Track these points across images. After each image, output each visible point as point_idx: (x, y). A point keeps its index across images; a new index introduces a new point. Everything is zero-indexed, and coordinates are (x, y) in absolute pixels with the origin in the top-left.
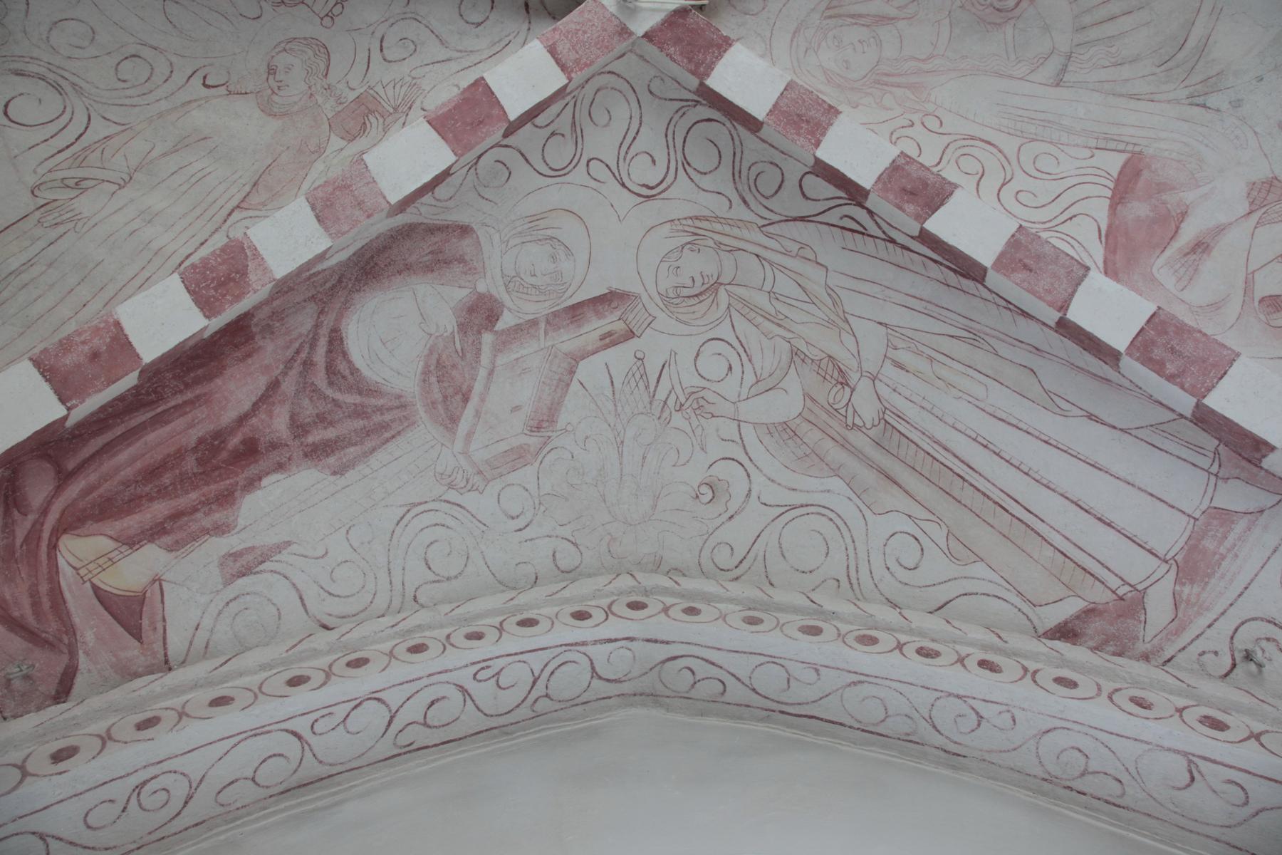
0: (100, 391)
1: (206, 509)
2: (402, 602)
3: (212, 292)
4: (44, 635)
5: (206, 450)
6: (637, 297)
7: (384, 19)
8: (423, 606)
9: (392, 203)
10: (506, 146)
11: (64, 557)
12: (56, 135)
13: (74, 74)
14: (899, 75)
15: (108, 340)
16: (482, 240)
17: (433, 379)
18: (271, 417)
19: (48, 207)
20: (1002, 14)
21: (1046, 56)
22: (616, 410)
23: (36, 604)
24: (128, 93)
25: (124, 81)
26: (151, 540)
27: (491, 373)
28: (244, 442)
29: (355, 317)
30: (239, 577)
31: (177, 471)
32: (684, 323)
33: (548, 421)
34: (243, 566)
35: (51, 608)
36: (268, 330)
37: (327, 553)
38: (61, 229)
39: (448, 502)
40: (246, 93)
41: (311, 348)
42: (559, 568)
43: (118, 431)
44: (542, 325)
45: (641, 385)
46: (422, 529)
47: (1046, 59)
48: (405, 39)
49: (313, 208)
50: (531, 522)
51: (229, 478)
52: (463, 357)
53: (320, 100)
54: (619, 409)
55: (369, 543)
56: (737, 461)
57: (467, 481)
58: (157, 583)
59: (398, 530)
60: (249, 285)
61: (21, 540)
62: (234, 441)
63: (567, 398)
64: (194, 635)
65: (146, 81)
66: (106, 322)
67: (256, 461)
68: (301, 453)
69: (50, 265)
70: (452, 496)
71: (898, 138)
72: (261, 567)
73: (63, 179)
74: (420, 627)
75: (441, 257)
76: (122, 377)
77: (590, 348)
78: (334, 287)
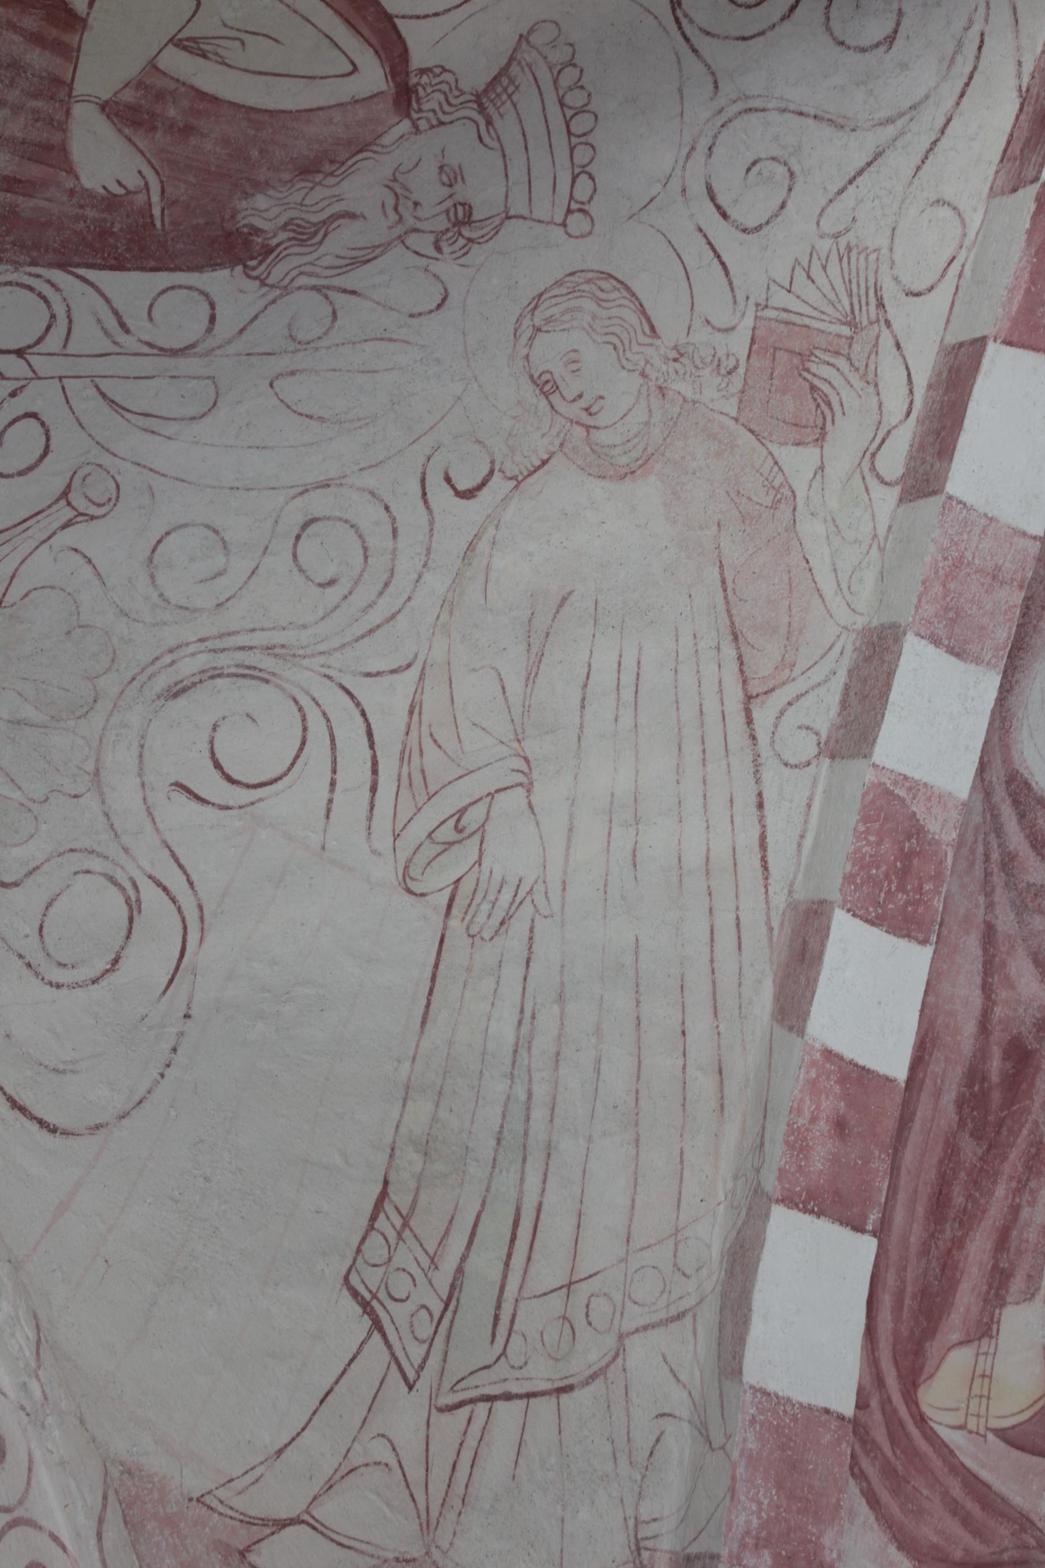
1: (1027, 1197)
4: (1006, 1556)
5: (972, 1111)
7: (685, 151)
9: (1042, 534)
11: (940, 1424)
12: (334, 762)
13: (253, 630)
15: (837, 1089)
18: (1012, 987)
19: (460, 903)
23: (966, 1521)
24: (360, 598)
25: (331, 583)
26: (1002, 1306)
28: (1006, 1056)
31: (963, 1175)
35: (983, 1509)
38: (519, 927)
40: (544, 463)
41: (998, 836)
48: (754, 163)
49: (936, 641)
51: (1023, 1126)
53: (684, 387)
60: (938, 843)
61: (889, 1445)
62: (995, 1066)
65: (366, 557)
66: (814, 1064)
69: (561, 998)
73: (430, 835)
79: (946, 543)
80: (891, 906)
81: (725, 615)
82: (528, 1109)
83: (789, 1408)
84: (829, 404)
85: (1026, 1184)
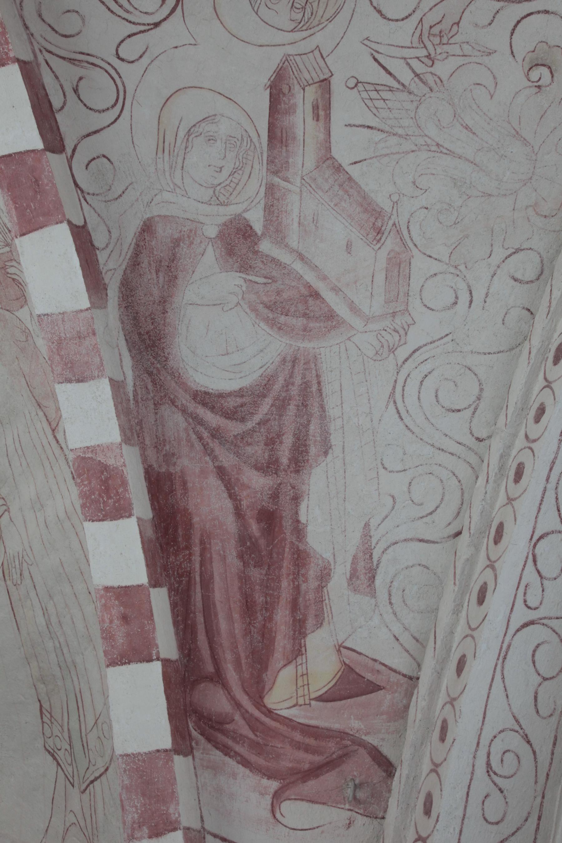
0: (154, 628)
1: (301, 579)
2: (476, 454)
3: (111, 501)
4: (334, 756)
5: (250, 556)
6: (287, 58)
8: (489, 437)
10: (74, 151)
11: (281, 709)
15: (117, 602)
16: (164, 212)
17: (282, 319)
18: (249, 488)
22: (400, 136)
23: (307, 749)
26: (305, 635)
27: (302, 257)
29: (191, 372)
30: (373, 582)
31: (257, 587)
32: (336, 13)
33: (376, 219)
34: (366, 574)
35: (316, 739)
36: (169, 458)
37: (393, 497)
38: (26, 574)
39: (406, 360)
41: (202, 425)
42: (532, 282)
43: (200, 619)
44: (276, 180)
45: (386, 95)
46: (419, 399)
49: (69, 381)
50: (469, 286)
51: (284, 548)
52: (274, 280)
54: (400, 131)
55: (405, 454)
56: (523, 18)
57: (395, 331)
58: (341, 649)
59: (407, 420)
61: (251, 733)
62: (255, 528)
63: (363, 186)
64: (402, 645)
66: (102, 597)
67: (281, 517)
68: (293, 475)
70: (402, 353)
72: (375, 559)
74: (503, 457)
75: (165, 263)
76: (151, 607)
77: (322, 136)
78: (154, 382)
79: (50, 336)
80: (108, 508)
81: (33, 398)
82: (62, 650)
83: (140, 758)
84: (20, 284)
85: (298, 574)
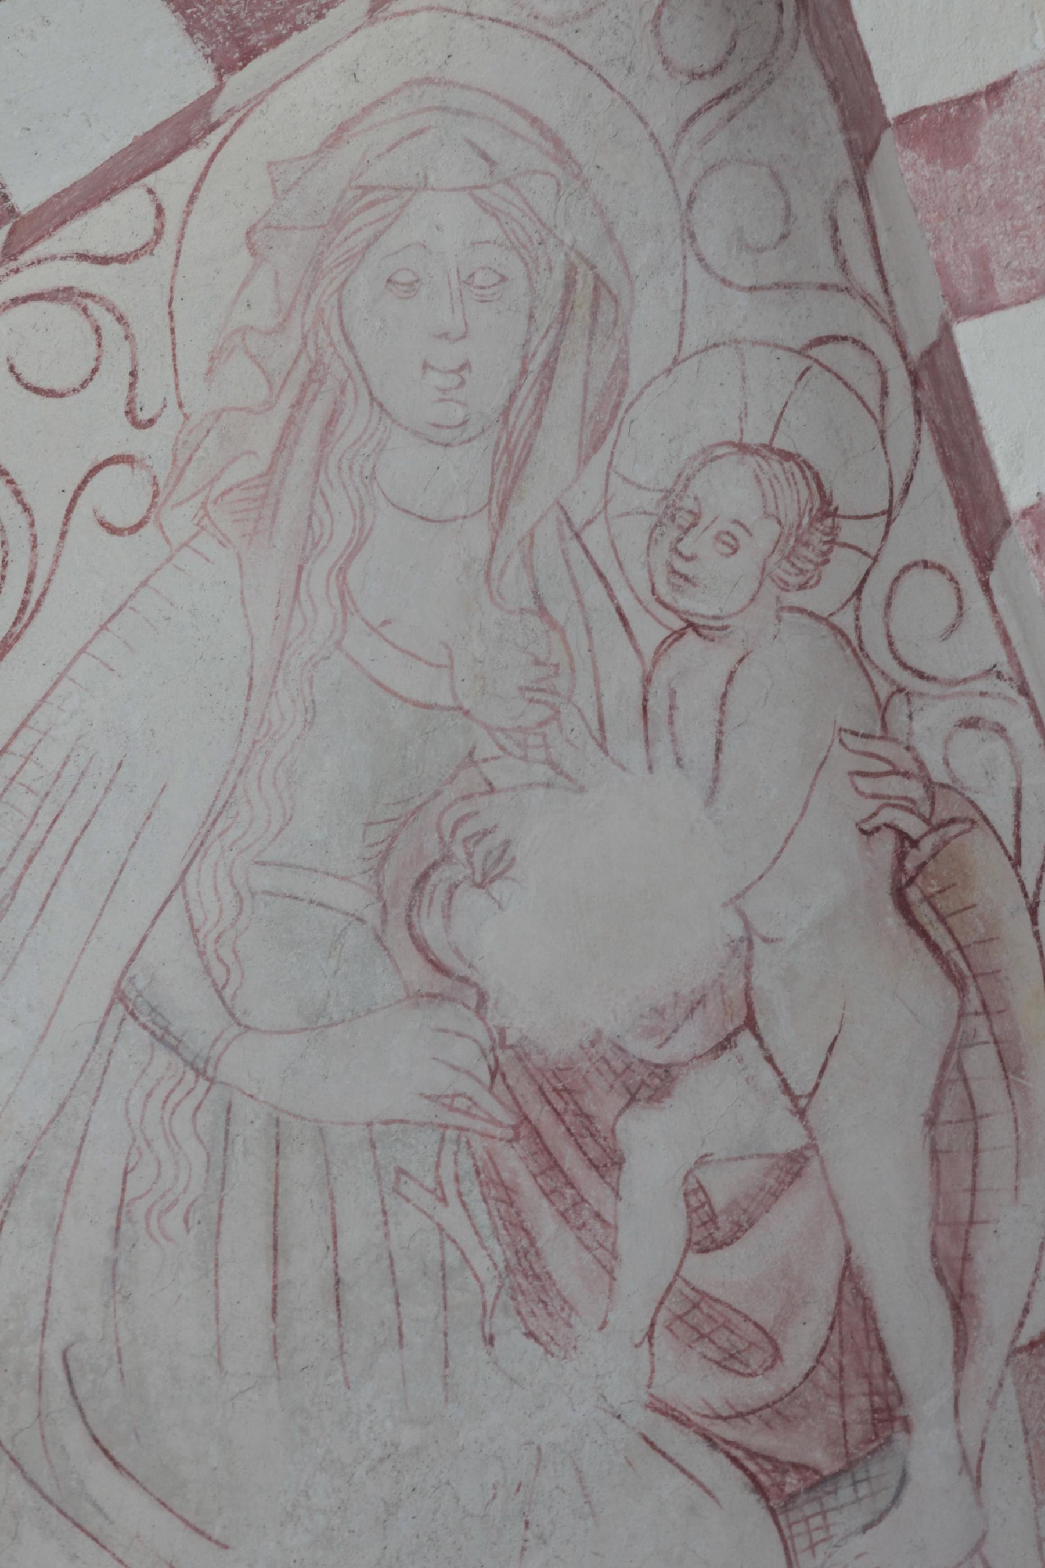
14: (319, 466)
20: (406, 888)
21: (228, 993)
47: (219, 993)
71: (97, 330)
